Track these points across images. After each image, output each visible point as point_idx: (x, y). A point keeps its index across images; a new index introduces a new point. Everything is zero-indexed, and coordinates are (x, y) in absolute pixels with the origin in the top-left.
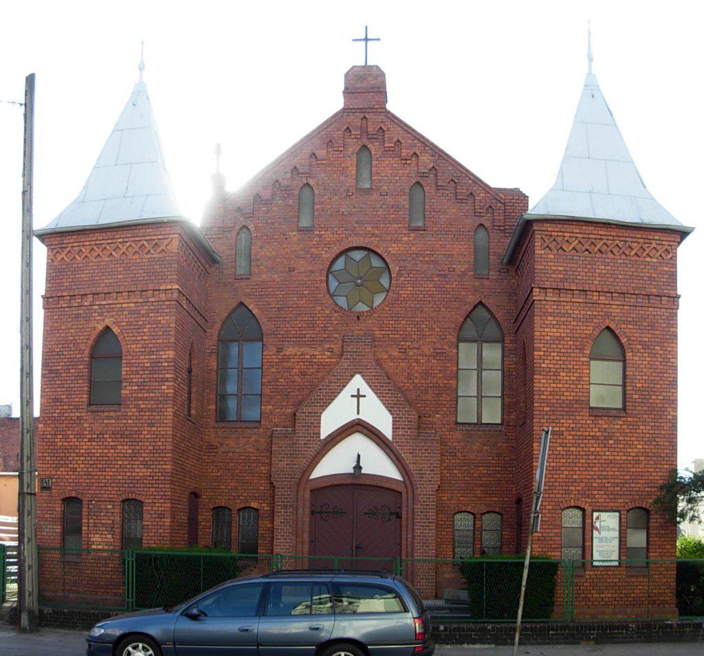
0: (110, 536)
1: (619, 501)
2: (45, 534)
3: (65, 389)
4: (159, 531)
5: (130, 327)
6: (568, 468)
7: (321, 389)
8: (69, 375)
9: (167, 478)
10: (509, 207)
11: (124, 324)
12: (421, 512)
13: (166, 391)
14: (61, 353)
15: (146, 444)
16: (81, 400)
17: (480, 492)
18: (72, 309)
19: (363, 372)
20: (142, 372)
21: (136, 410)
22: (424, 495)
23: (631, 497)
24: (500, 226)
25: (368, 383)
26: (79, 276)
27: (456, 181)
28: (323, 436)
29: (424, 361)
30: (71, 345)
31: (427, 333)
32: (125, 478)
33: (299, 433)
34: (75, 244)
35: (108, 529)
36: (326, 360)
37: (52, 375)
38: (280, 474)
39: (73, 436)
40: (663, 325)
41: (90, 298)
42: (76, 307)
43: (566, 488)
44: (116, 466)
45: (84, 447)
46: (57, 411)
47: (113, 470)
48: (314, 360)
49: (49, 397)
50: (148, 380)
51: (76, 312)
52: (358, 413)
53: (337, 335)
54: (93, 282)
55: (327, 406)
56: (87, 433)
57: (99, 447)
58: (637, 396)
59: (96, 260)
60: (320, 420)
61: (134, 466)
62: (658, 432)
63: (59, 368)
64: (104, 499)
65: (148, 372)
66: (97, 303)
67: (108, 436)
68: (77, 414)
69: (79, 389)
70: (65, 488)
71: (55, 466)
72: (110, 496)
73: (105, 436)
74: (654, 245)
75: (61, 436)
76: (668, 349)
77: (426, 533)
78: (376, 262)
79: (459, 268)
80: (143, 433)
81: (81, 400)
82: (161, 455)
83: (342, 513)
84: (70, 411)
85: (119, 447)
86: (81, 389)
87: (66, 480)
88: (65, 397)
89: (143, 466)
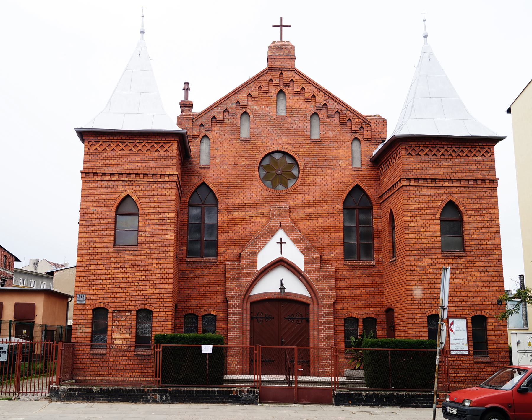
1: (465, 311)
3: (97, 234)
4: (164, 331)
5: (144, 196)
6: (430, 290)
7: (257, 238)
8: (100, 225)
9: (169, 295)
10: (374, 127)
11: (141, 194)
12: (324, 317)
14: (95, 210)
15: (155, 272)
17: (361, 304)
18: (103, 182)
19: (284, 228)
21: (146, 250)
22: (325, 306)
23: (474, 308)
24: (368, 138)
25: (287, 234)
27: (340, 112)
29: (322, 221)
31: (324, 204)
32: (140, 294)
33: (244, 266)
36: (259, 220)
38: (231, 293)
40: (487, 198)
41: (116, 176)
42: (106, 181)
43: (430, 302)
44: (133, 287)
45: (111, 273)
47: (131, 289)
48: (252, 220)
51: (106, 184)
52: (281, 253)
54: (119, 166)
55: (261, 249)
56: (113, 264)
57: (121, 274)
58: (473, 243)
59: (121, 152)
62: (489, 265)
63: (93, 220)
64: (124, 309)
66: (121, 179)
67: (128, 266)
68: (106, 251)
70: (95, 301)
72: (129, 307)
76: (492, 212)
77: (327, 331)
78: (289, 161)
79: (342, 164)
80: (153, 265)
81: (109, 242)
82: (167, 280)
83: (270, 318)
84: (101, 249)
85: (136, 274)
86: (109, 235)
87: (96, 296)
89: (153, 287)
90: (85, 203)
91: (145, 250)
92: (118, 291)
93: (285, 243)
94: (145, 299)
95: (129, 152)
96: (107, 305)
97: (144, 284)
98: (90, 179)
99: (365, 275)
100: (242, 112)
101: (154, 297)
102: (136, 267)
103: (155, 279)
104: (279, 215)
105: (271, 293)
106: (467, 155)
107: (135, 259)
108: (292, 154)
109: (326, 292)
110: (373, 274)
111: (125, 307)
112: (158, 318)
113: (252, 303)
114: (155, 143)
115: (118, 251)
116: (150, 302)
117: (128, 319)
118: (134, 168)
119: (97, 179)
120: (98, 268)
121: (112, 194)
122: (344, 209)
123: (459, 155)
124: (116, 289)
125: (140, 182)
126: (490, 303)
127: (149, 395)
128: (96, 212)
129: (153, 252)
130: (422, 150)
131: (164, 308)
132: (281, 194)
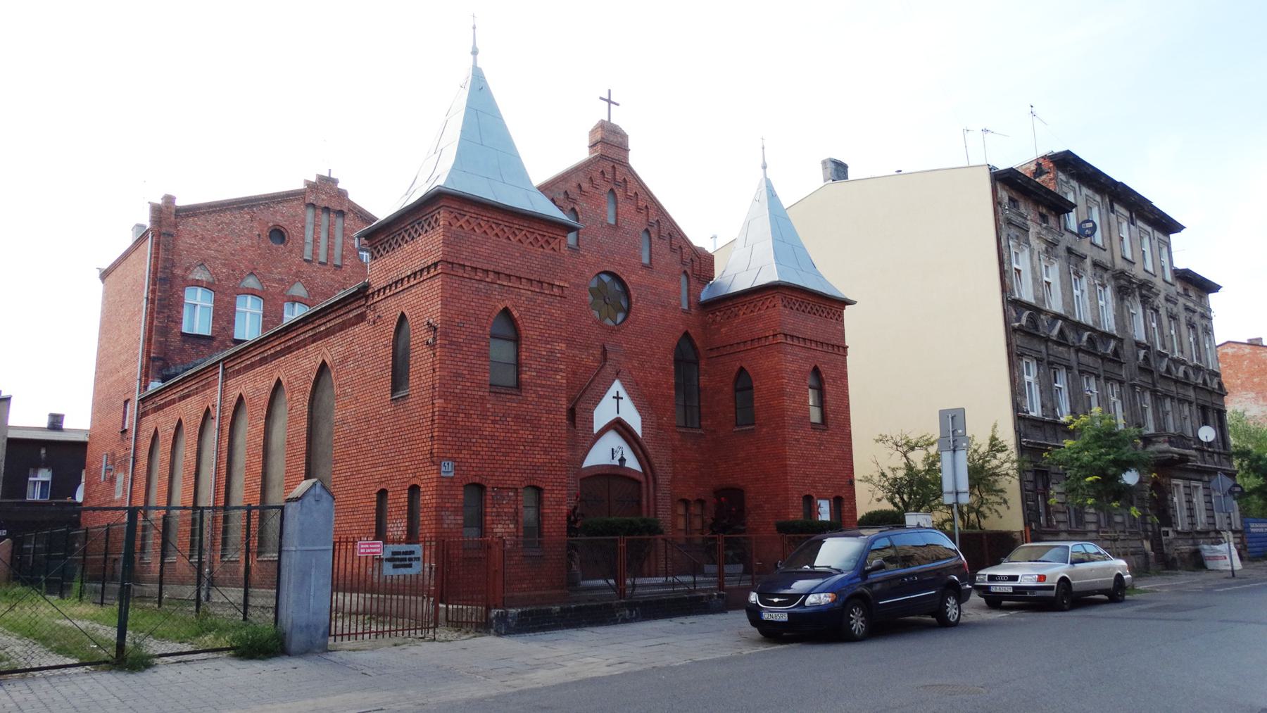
0: (512, 526)
2: (446, 526)
4: (558, 518)
7: (592, 389)
12: (662, 499)
13: (560, 381)
16: (484, 378)
18: (473, 281)
20: (539, 359)
21: (533, 395)
25: (624, 387)
26: (477, 249)
28: (596, 430)
30: (473, 319)
32: (527, 463)
34: (473, 215)
35: (511, 518)
37: (453, 347)
39: (475, 416)
41: (491, 276)
42: (476, 280)
48: (584, 363)
50: (545, 368)
51: (477, 286)
52: (618, 413)
53: (597, 343)
55: (597, 404)
57: (501, 431)
59: (494, 238)
60: (593, 416)
61: (536, 452)
63: (462, 340)
64: (507, 486)
65: (544, 360)
66: (498, 282)
67: (510, 419)
68: (479, 393)
69: (481, 366)
71: (456, 447)
72: (514, 482)
73: (508, 419)
74: (833, 311)
75: (463, 415)
78: (617, 288)
80: (542, 419)
81: (484, 378)
85: (521, 432)
88: (467, 372)
89: (542, 453)
90: (448, 311)
91: (531, 397)
93: (622, 398)
94: (533, 471)
95: (505, 241)
96: (484, 480)
97: (532, 448)
98: (456, 274)
99: (695, 447)
100: (569, 208)
101: (545, 468)
102: (521, 420)
104: (614, 360)
105: (603, 466)
106: (826, 317)
107: (518, 409)
108: (624, 278)
109: (663, 467)
110: (702, 445)
112: (551, 499)
113: (581, 480)
114: (539, 234)
115: (498, 395)
116: (541, 476)
117: (512, 502)
118: (513, 268)
119: (465, 275)
120: (470, 420)
121: (486, 302)
122: (675, 360)
123: (820, 315)
124: (495, 454)
125: (523, 291)
126: (844, 483)
127: (618, 611)
128: (464, 329)
129: (540, 400)
130: (794, 303)
131: (558, 484)
132: (614, 332)
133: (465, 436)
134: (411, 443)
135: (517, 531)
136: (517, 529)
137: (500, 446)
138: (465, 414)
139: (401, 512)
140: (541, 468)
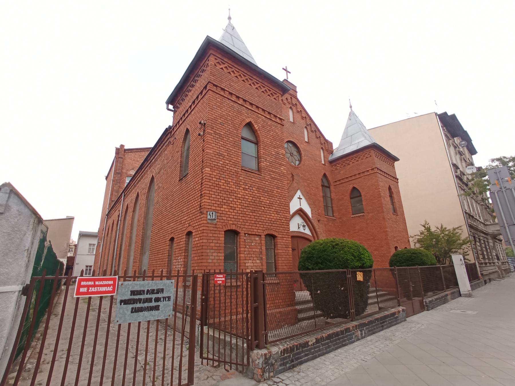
3: (226, 149)
37: (217, 136)
44: (261, 210)
46: (220, 162)
49: (214, 150)
61: (271, 212)
63: (221, 133)
69: (236, 152)
72: (259, 231)
73: (254, 189)
75: (224, 182)
84: (230, 165)
85: (262, 198)
86: (237, 153)
89: (275, 213)
92: (247, 213)
97: (269, 209)
101: (278, 223)
103: (276, 206)
111: (255, 231)
115: (246, 172)
120: (229, 185)
124: (245, 210)
133: (225, 196)
134: (188, 204)
135: (262, 265)
136: (262, 263)
137: (249, 205)
138: (225, 181)
139: (181, 252)
140: (275, 223)
